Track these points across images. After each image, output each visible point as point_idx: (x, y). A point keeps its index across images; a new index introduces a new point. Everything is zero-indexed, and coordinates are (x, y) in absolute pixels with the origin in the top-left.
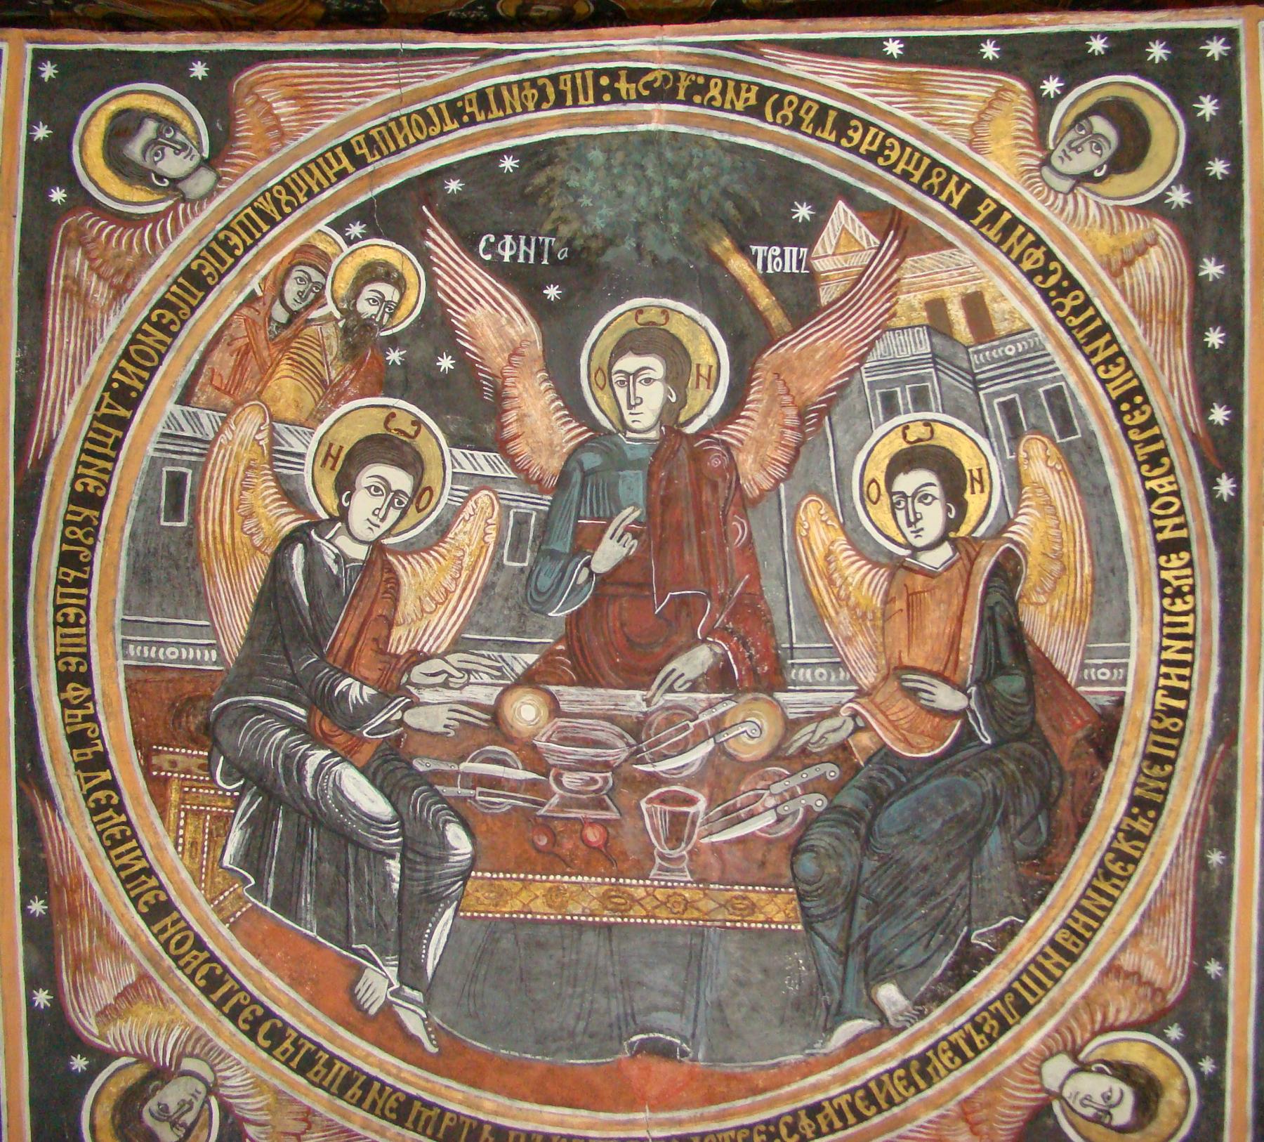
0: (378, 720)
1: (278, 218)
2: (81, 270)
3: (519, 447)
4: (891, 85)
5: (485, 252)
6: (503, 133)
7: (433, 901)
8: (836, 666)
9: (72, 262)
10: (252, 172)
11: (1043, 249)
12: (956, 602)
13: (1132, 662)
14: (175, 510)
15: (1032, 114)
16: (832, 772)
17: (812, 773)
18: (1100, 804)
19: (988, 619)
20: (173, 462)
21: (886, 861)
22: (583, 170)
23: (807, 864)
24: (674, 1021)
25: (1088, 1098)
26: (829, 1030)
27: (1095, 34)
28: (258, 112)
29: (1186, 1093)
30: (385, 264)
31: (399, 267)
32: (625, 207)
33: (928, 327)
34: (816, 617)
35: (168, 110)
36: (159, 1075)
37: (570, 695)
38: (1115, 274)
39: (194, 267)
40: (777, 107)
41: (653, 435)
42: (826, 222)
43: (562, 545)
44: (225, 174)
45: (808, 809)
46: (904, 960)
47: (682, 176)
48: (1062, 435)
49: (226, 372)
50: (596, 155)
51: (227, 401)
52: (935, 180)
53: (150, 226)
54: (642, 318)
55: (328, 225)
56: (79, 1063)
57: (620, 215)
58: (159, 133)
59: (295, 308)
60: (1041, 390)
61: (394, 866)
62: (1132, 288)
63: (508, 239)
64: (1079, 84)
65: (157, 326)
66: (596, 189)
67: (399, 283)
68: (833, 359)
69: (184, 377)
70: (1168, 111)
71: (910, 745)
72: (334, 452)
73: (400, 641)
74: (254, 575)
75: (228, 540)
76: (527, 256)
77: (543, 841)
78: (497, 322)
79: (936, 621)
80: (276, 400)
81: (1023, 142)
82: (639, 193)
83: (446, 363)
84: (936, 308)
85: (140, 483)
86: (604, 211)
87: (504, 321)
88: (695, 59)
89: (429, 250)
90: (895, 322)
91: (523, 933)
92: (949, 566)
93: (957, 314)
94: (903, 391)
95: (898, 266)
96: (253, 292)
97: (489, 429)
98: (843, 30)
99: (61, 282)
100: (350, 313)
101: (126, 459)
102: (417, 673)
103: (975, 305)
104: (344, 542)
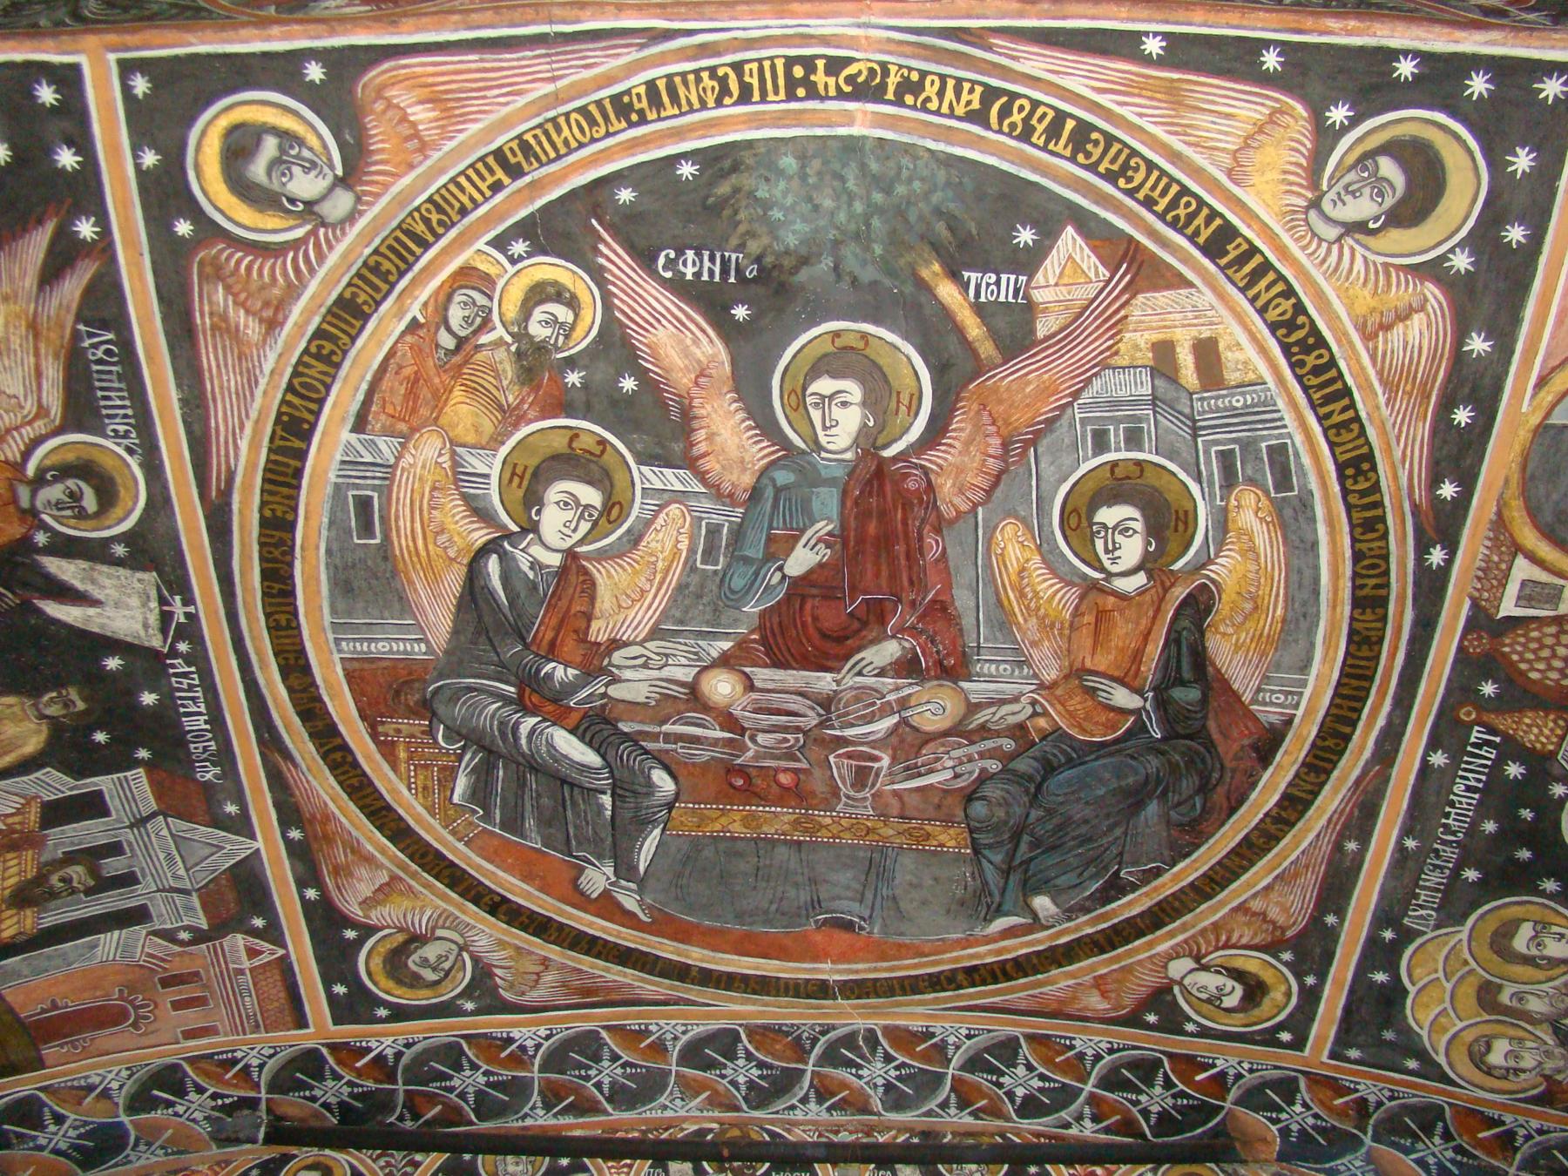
0: (583, 694)
1: (431, 239)
2: (226, 306)
3: (708, 464)
4: (1144, 93)
5: (665, 268)
6: (678, 134)
7: (643, 824)
8: (1020, 664)
9: (214, 298)
10: (395, 190)
11: (1293, 300)
12: (1144, 622)
13: (1307, 692)
14: (366, 528)
15: (1309, 145)
16: (1008, 744)
17: (989, 744)
18: (1254, 796)
19: (1173, 640)
20: (357, 487)
21: (1050, 812)
22: (773, 177)
23: (979, 809)
24: (855, 906)
25: (1205, 987)
26: (988, 920)
27: (1406, 53)
28: (391, 120)
29: (1288, 994)
30: (555, 283)
31: (571, 287)
32: (822, 223)
33: (1152, 369)
34: (1003, 622)
35: (287, 123)
36: (417, 939)
37: (764, 676)
38: (1368, 337)
39: (347, 295)
40: (1005, 112)
41: (849, 456)
42: (1051, 248)
43: (755, 551)
44: (365, 193)
45: (983, 770)
46: (1058, 881)
47: (888, 191)
48: (1277, 490)
49: (398, 400)
50: (789, 162)
51: (403, 427)
52: (1182, 212)
53: (291, 254)
54: (838, 342)
55: (487, 243)
56: (350, 934)
57: (817, 230)
59: (463, 333)
60: (1263, 445)
61: (606, 800)
63: (690, 254)
64: (1372, 115)
65: (318, 357)
66: (789, 201)
67: (573, 303)
68: (1047, 391)
69: (355, 407)
70: (1473, 159)
71: (1083, 731)
72: (519, 470)
73: (599, 631)
74: (453, 581)
75: (423, 553)
76: (711, 273)
77: (740, 782)
78: (681, 342)
79: (1123, 631)
80: (454, 426)
81: (1292, 178)
82: (838, 208)
83: (628, 384)
84: (1164, 351)
85: (327, 507)
86: (799, 226)
87: (689, 342)
88: (908, 50)
89: (602, 267)
91: (722, 846)
92: (1142, 592)
93: (1186, 358)
94: (1116, 430)
95: (1127, 303)
96: (414, 319)
97: (677, 447)
98: (1093, 18)
99: (207, 321)
100: (522, 336)
101: (310, 485)
102: (617, 657)
103: (1207, 352)
104: (537, 551)
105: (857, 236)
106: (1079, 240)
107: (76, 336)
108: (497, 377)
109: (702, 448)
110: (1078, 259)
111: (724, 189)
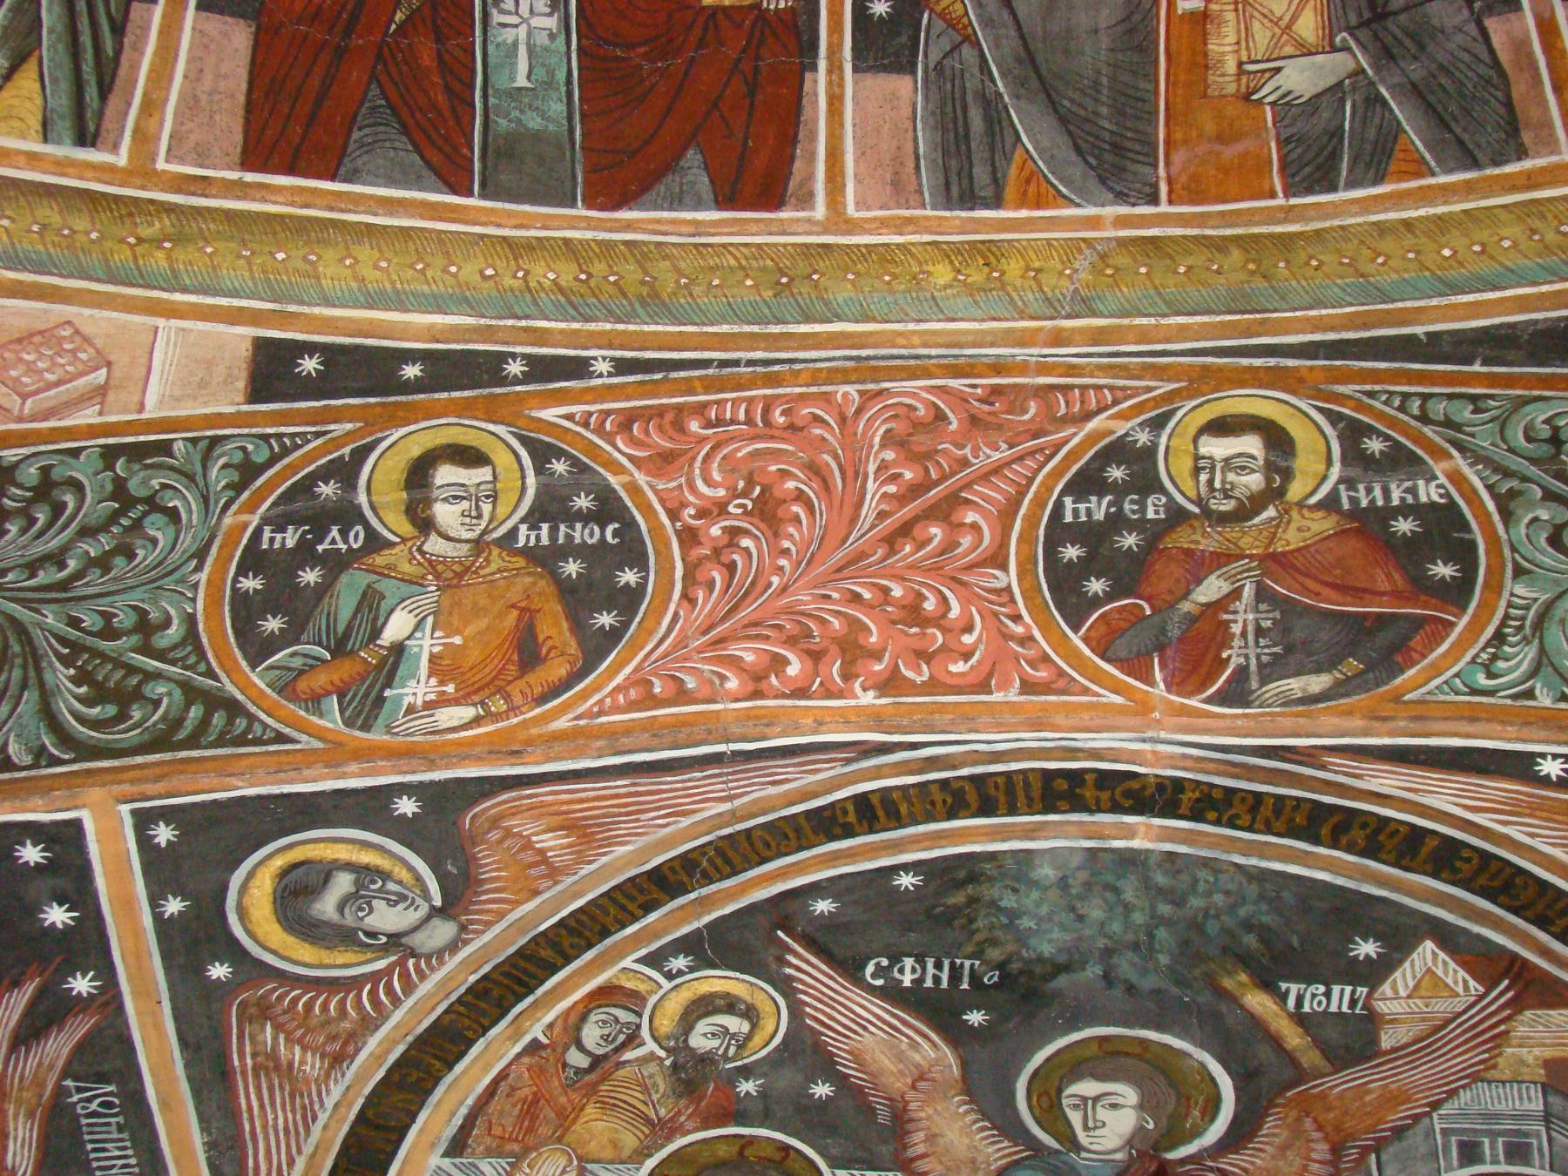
4: (1538, 813)
9: (260, 1038)
22: (1023, 888)
28: (509, 849)
31: (748, 998)
32: (1088, 932)
35: (367, 858)
41: (1119, 1156)
42: (1401, 962)
44: (472, 922)
47: (1179, 902)
49: (509, 1122)
51: (516, 1147)
53: (368, 987)
57: (1080, 939)
58: (359, 885)
59: (600, 1051)
63: (909, 962)
66: (1044, 910)
69: (451, 1130)
76: (937, 979)
82: (1110, 919)
86: (1056, 934)
88: (1211, 766)
89: (791, 978)
90: (1492, 1074)
98: (1468, 736)
99: (249, 1061)
105: (1136, 946)
106: (1442, 955)
107: (60, 1092)
108: (645, 1089)
109: (921, 1149)
110: (1440, 972)
111: (958, 898)
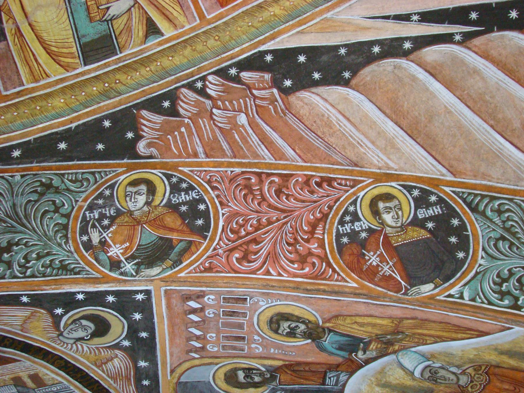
27: (79, 293)
33: (15, 385)
62: (107, 370)
64: (72, 310)
70: (118, 318)
